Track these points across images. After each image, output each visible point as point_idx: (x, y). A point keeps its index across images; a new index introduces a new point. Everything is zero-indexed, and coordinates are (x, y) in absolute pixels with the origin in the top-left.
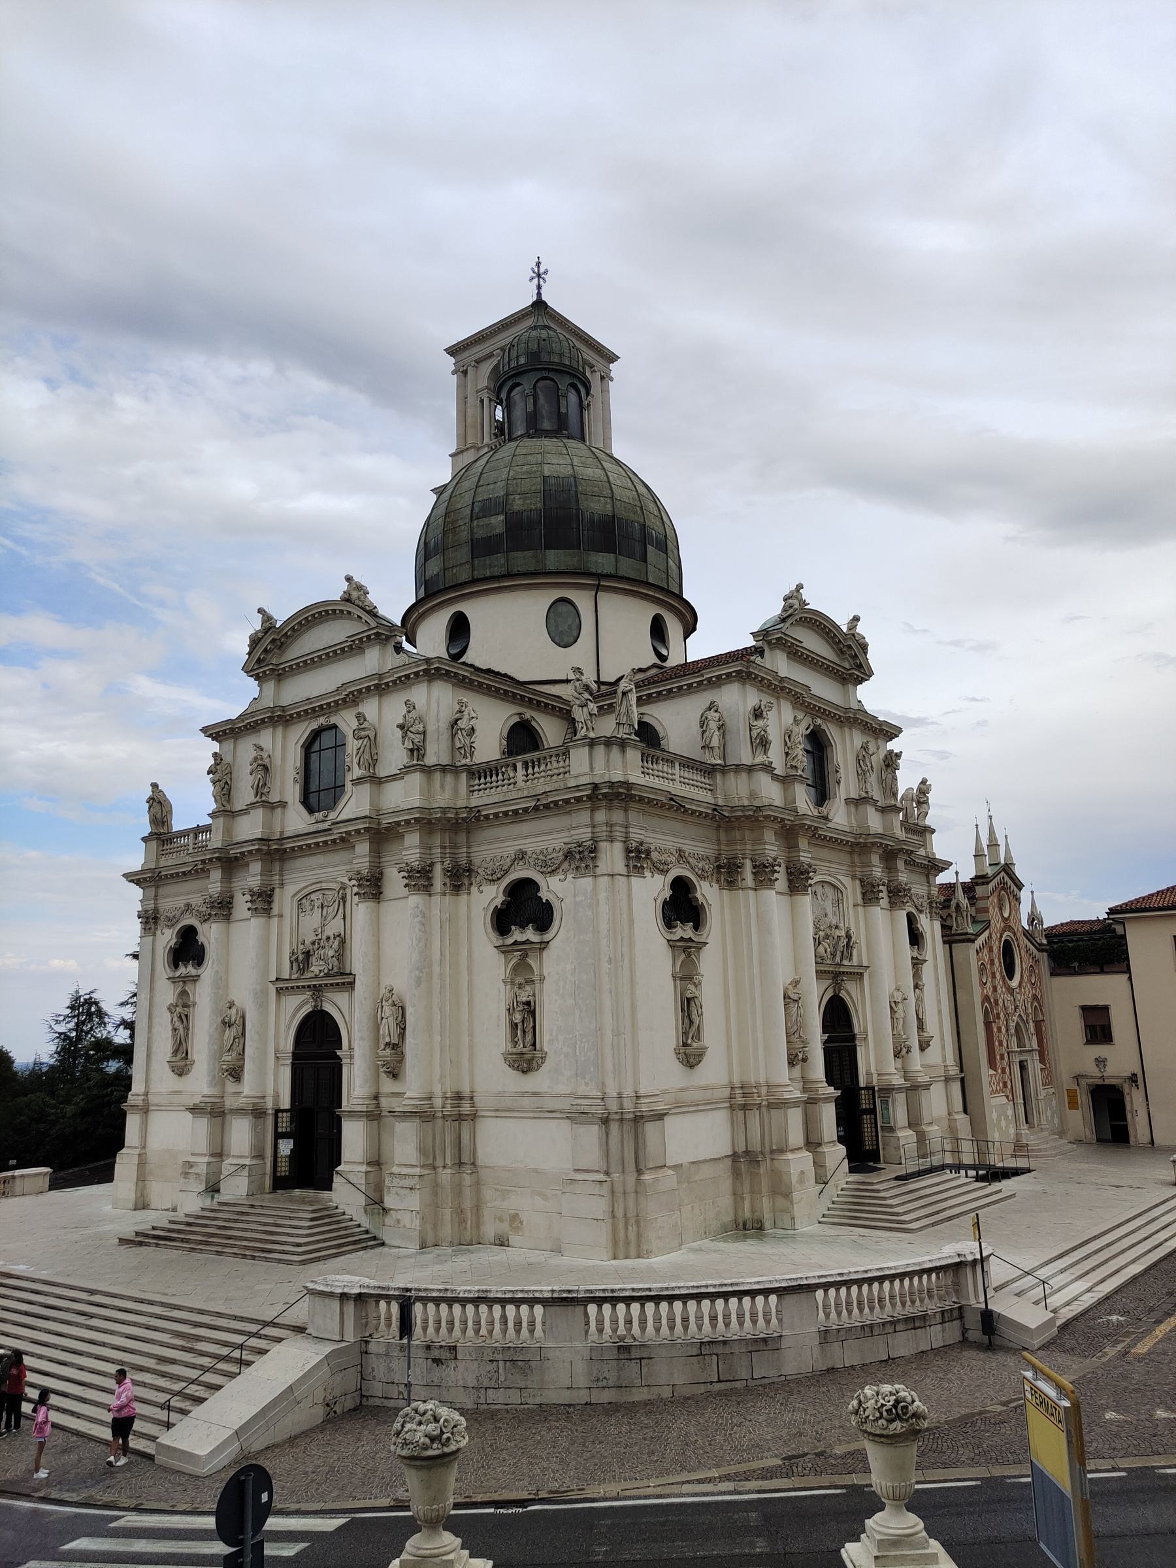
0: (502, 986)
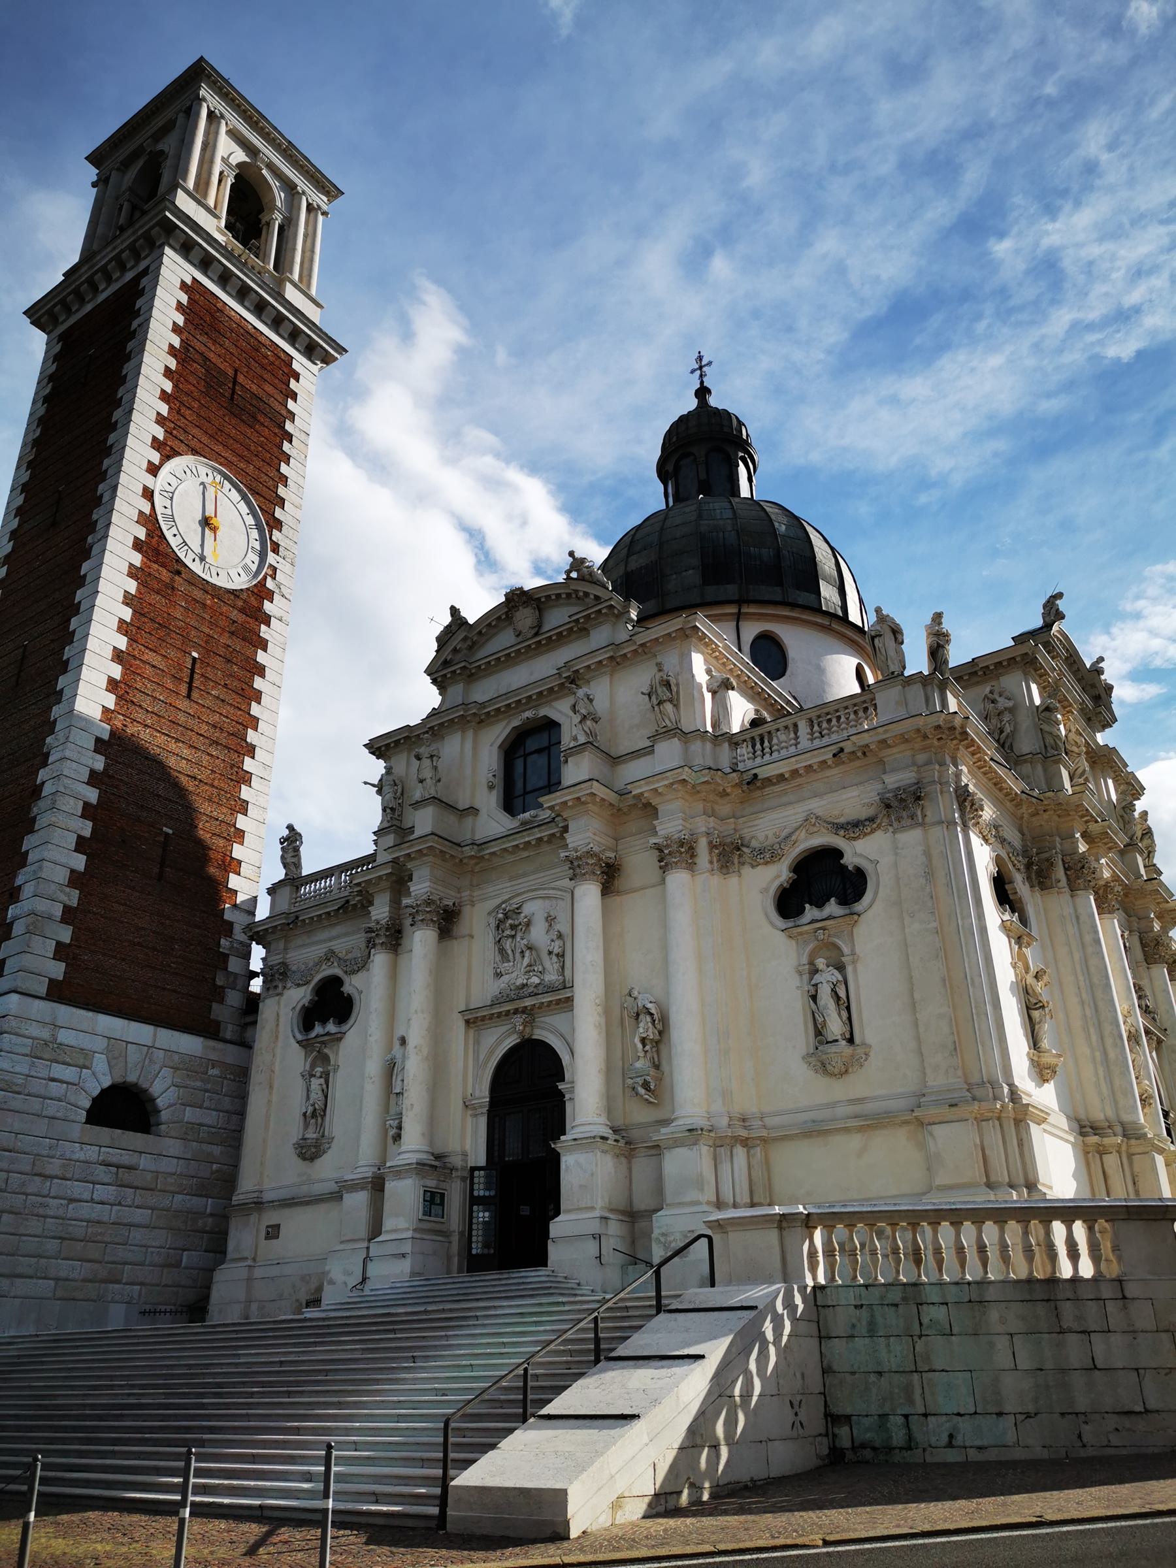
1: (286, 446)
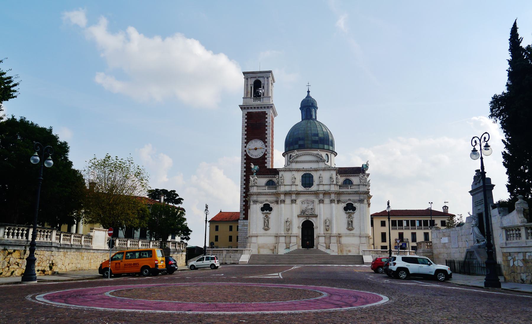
0: (346, 219)
1: (266, 128)
